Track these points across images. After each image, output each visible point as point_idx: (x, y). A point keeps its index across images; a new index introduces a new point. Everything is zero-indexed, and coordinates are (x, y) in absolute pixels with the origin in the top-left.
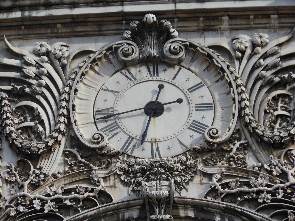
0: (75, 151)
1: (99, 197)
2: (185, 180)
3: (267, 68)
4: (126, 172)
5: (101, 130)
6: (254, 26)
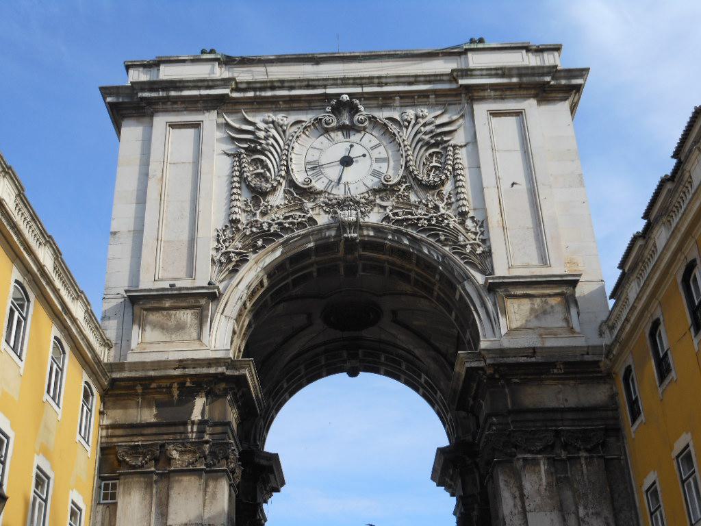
0: (292, 190)
3: (425, 134)
4: (327, 205)
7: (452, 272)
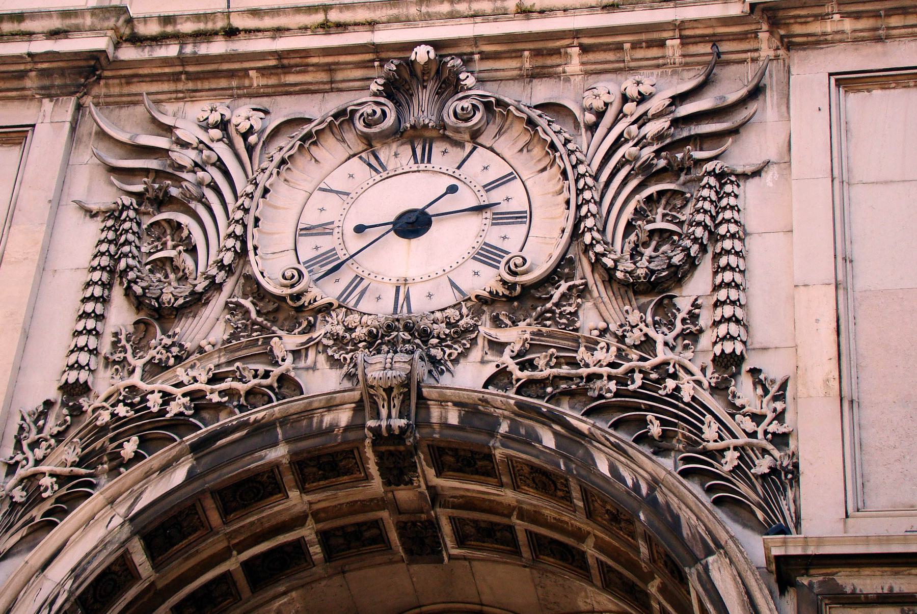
0: (247, 303)
1: (279, 388)
2: (450, 355)
3: (641, 143)
4: (339, 341)
5: (304, 263)
6: (633, 64)
7: (675, 523)
